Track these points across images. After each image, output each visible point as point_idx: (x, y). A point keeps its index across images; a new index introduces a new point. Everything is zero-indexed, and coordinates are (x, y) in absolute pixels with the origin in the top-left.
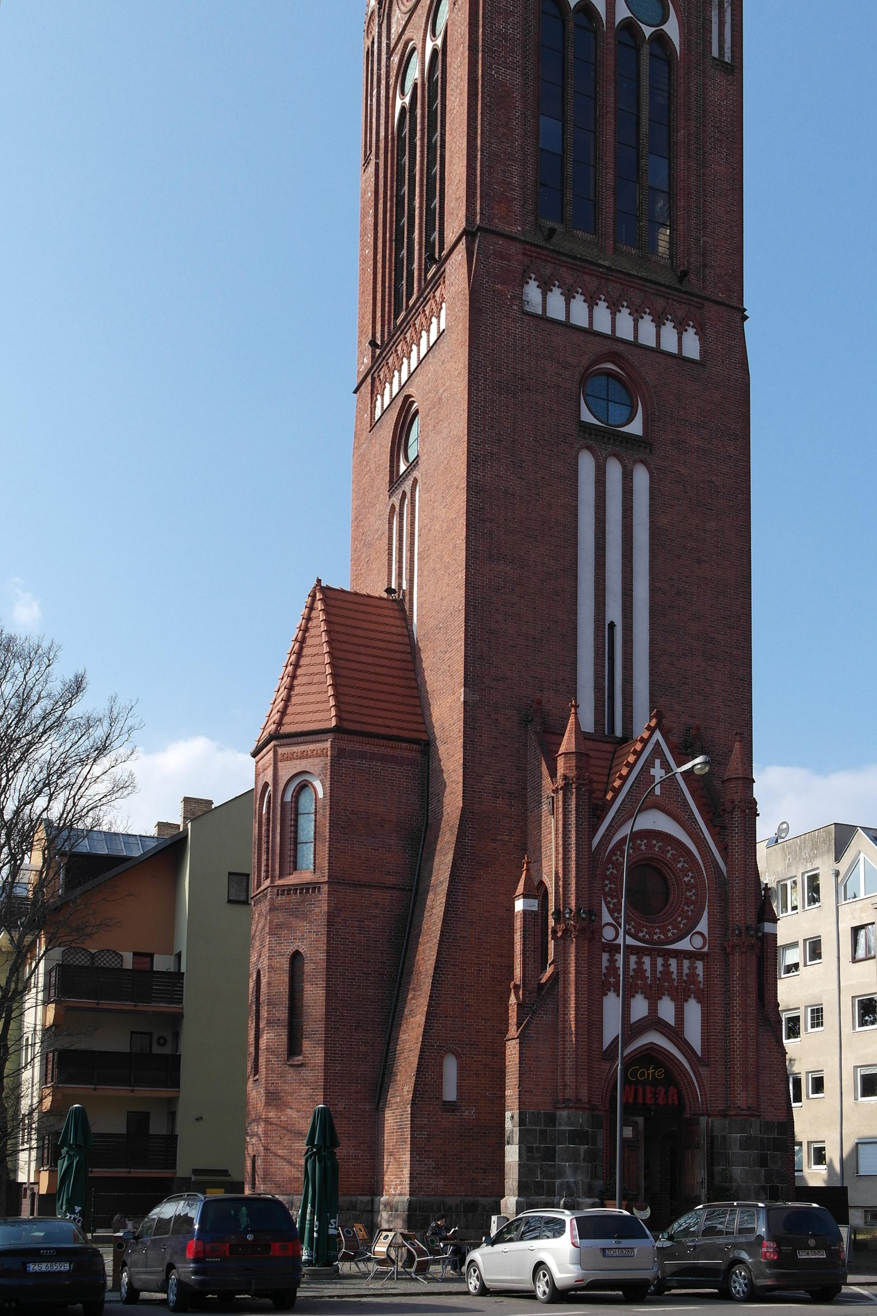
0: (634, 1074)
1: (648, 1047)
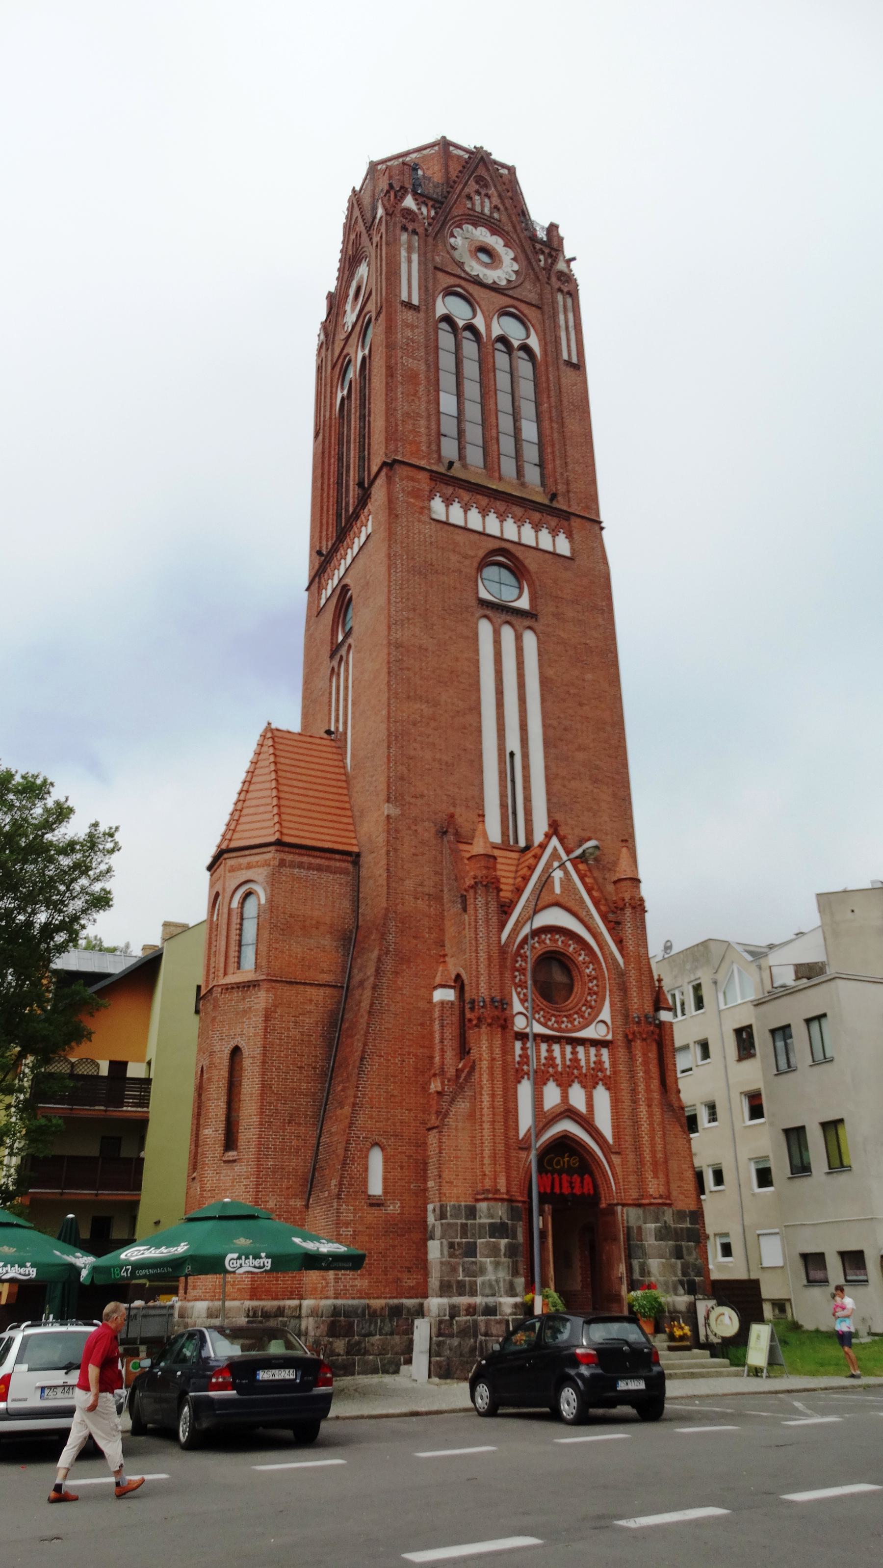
0: (550, 1163)
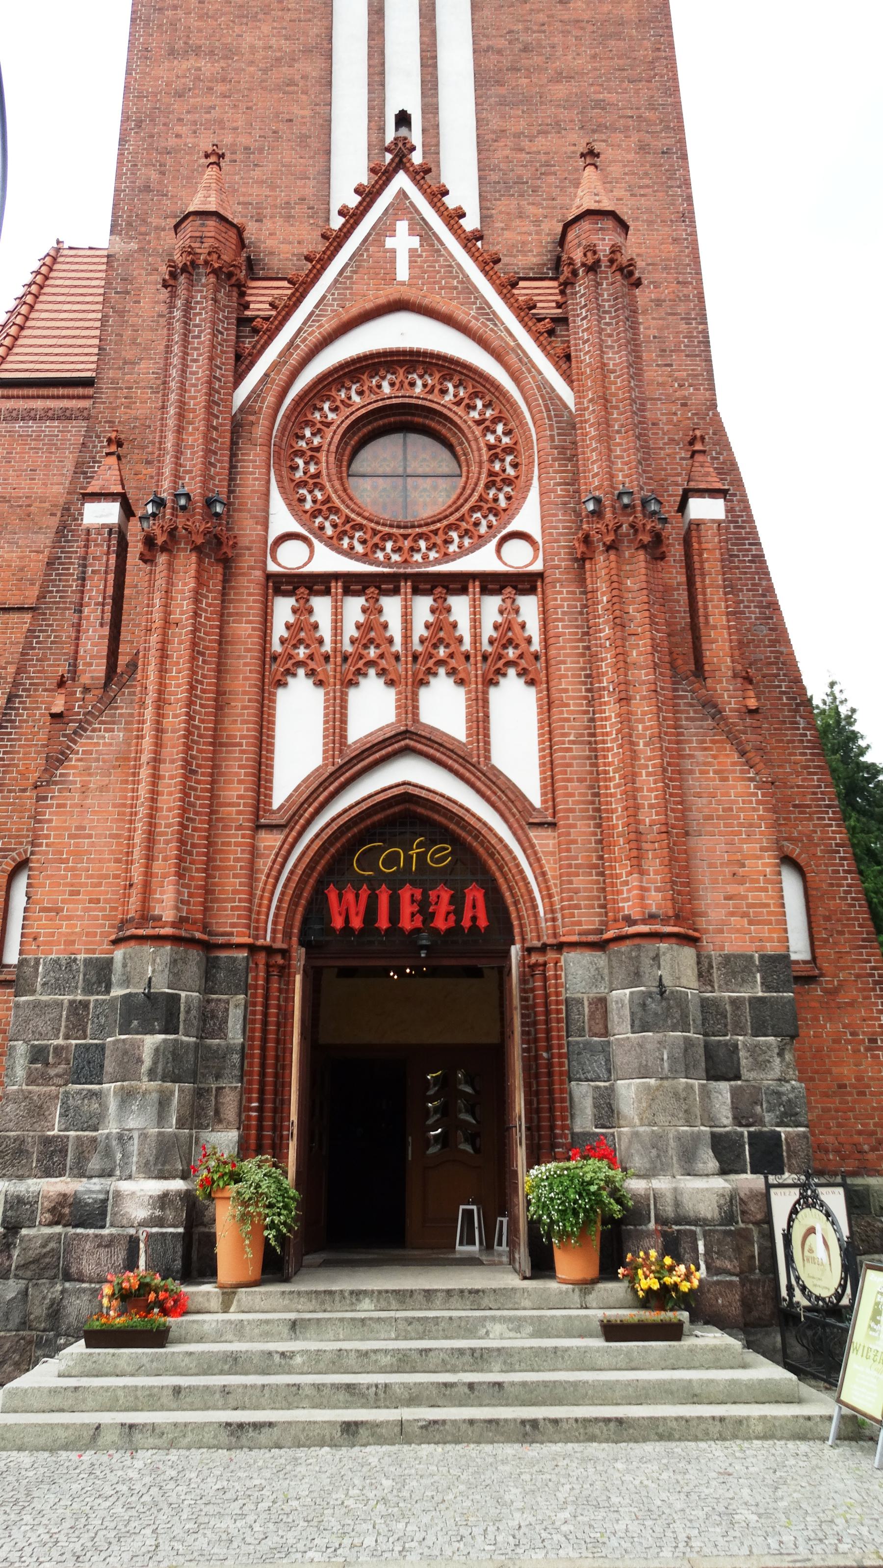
1: (396, 791)
